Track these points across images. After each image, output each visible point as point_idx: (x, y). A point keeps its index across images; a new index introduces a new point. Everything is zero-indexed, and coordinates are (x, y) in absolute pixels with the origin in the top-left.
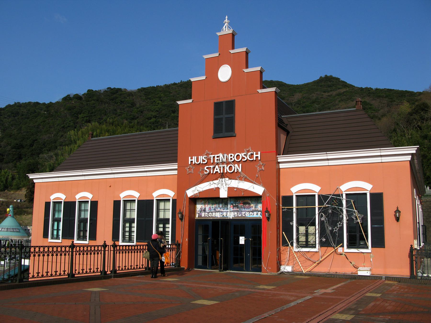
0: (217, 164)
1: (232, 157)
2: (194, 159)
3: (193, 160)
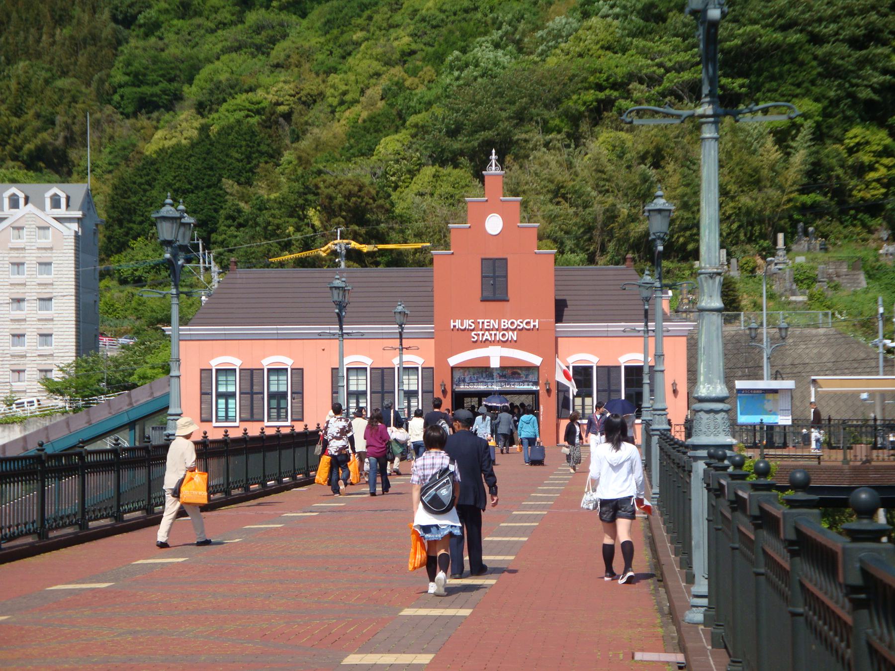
0: (487, 330)
1: (506, 323)
2: (458, 324)
3: (456, 324)
